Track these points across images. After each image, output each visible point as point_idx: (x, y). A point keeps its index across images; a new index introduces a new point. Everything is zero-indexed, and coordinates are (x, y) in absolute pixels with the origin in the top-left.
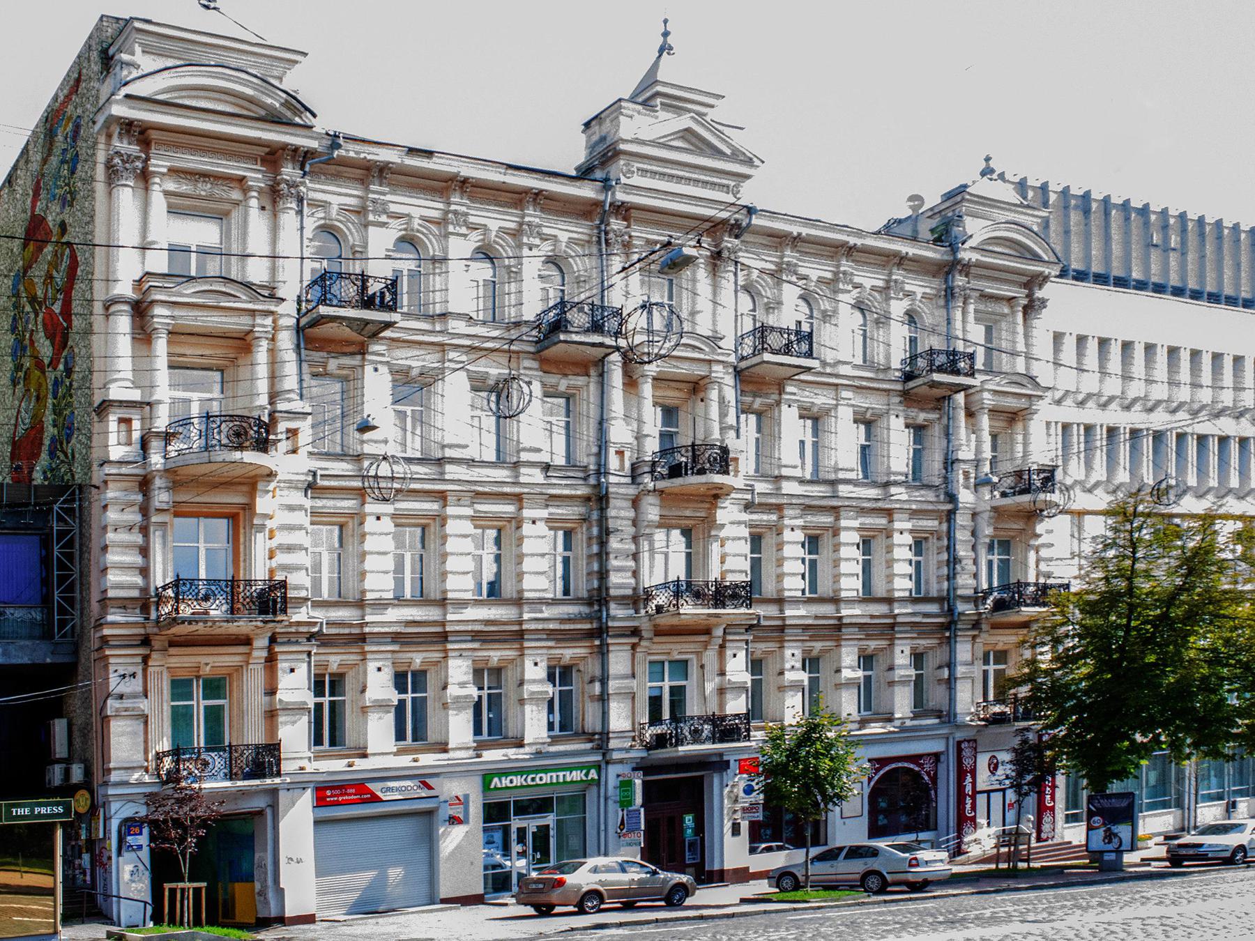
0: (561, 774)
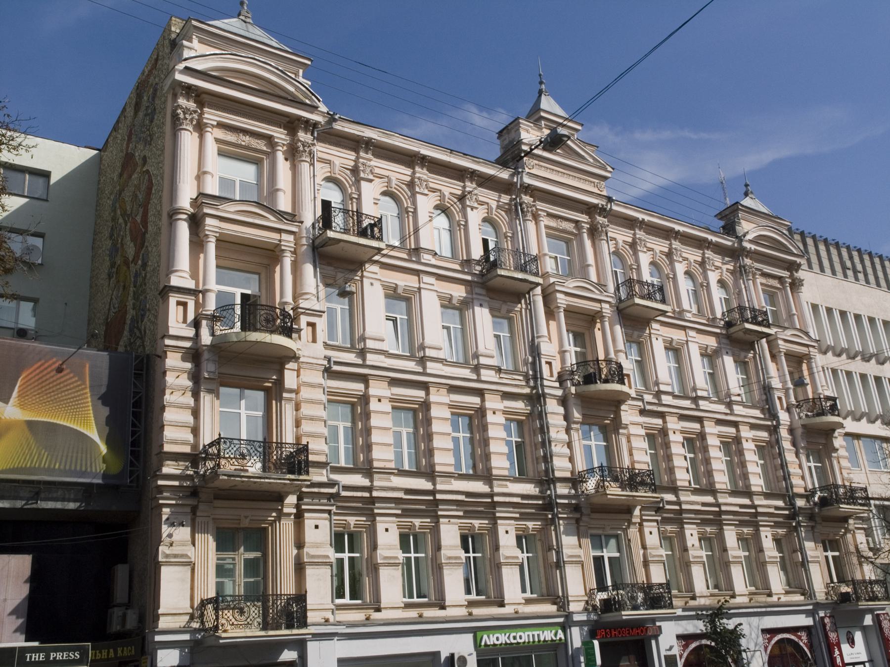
0: (536, 633)
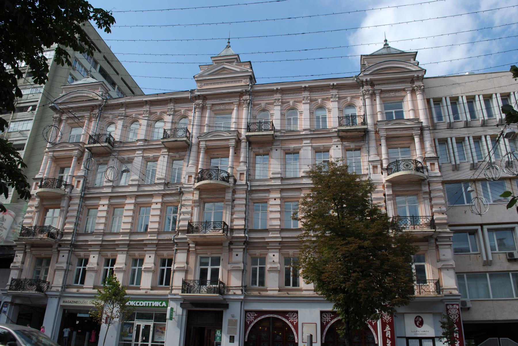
0: (150, 302)
